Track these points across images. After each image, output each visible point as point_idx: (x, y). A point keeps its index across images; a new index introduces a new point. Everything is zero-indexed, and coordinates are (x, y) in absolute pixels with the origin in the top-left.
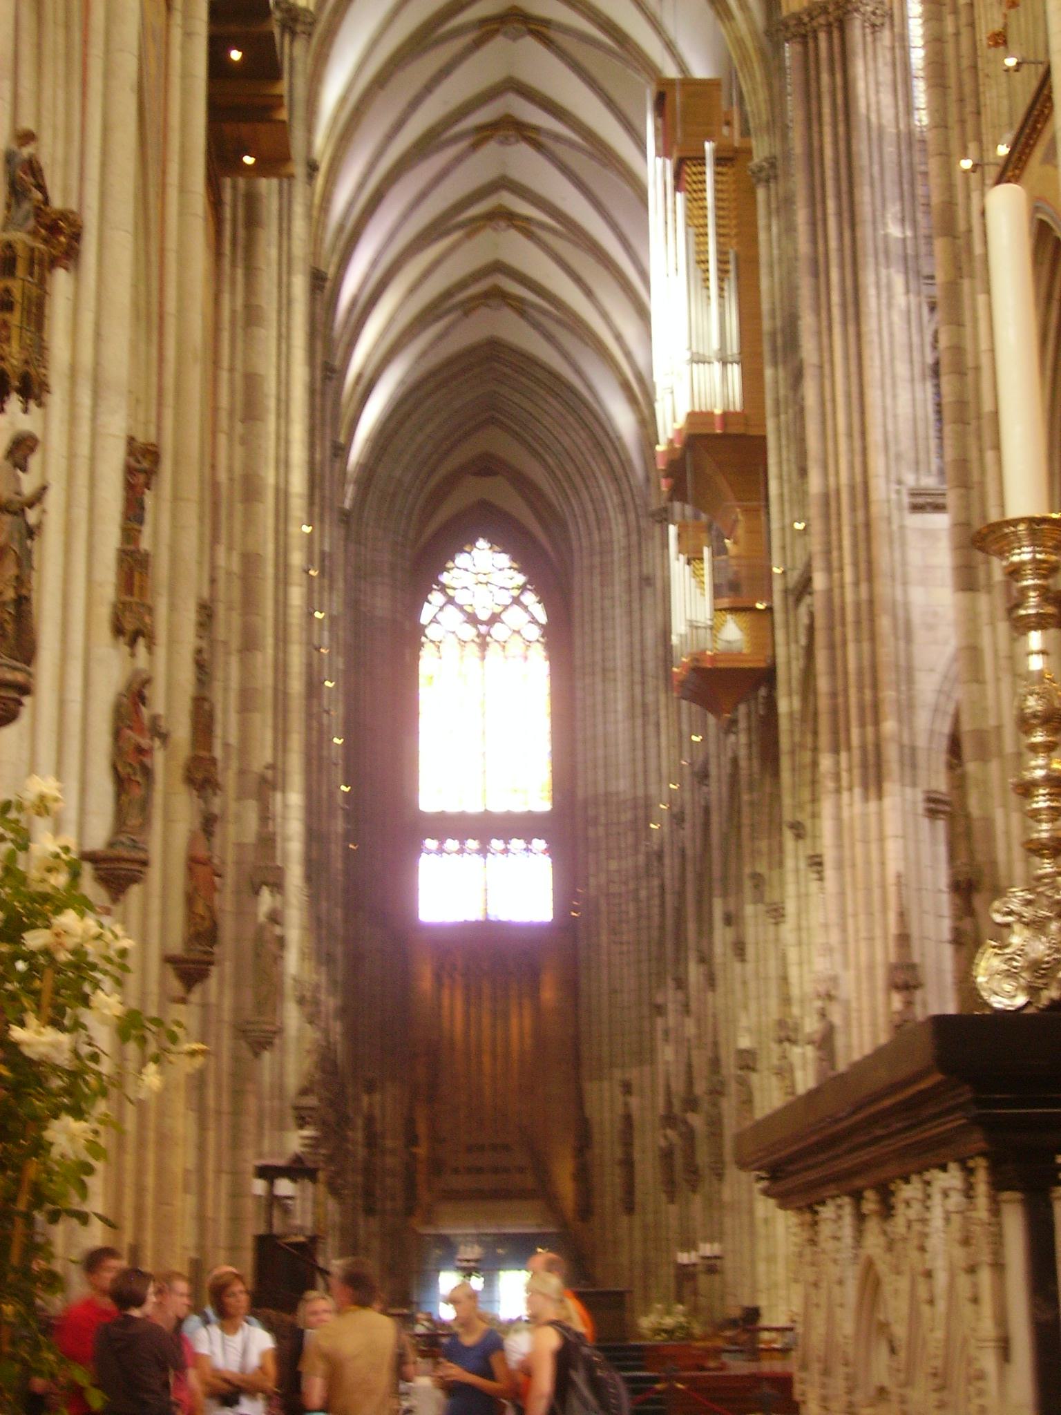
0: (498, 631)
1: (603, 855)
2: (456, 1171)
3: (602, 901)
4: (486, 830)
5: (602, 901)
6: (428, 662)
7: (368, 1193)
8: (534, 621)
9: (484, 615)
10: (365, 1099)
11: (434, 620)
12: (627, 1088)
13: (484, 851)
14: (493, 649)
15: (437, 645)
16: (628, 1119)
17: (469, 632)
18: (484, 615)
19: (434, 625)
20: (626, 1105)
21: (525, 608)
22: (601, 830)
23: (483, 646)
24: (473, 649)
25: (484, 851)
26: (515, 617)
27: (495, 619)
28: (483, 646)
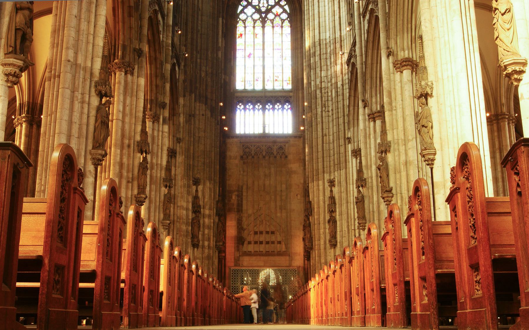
0: (270, 16)
1: (318, 70)
2: (250, 243)
3: (318, 92)
4: (265, 99)
5: (318, 92)
6: (240, 28)
7: (194, 236)
8: (285, 11)
9: (263, 9)
10: (194, 187)
11: (242, 11)
12: (332, 183)
13: (264, 109)
14: (268, 23)
15: (244, 21)
16: (332, 198)
17: (257, 16)
18: (263, 9)
19: (243, 14)
20: (331, 191)
21: (282, 7)
22: (317, 58)
23: (264, 21)
24: (259, 23)
25: (264, 109)
26: (277, 10)
27: (268, 11)
28: (264, 21)
